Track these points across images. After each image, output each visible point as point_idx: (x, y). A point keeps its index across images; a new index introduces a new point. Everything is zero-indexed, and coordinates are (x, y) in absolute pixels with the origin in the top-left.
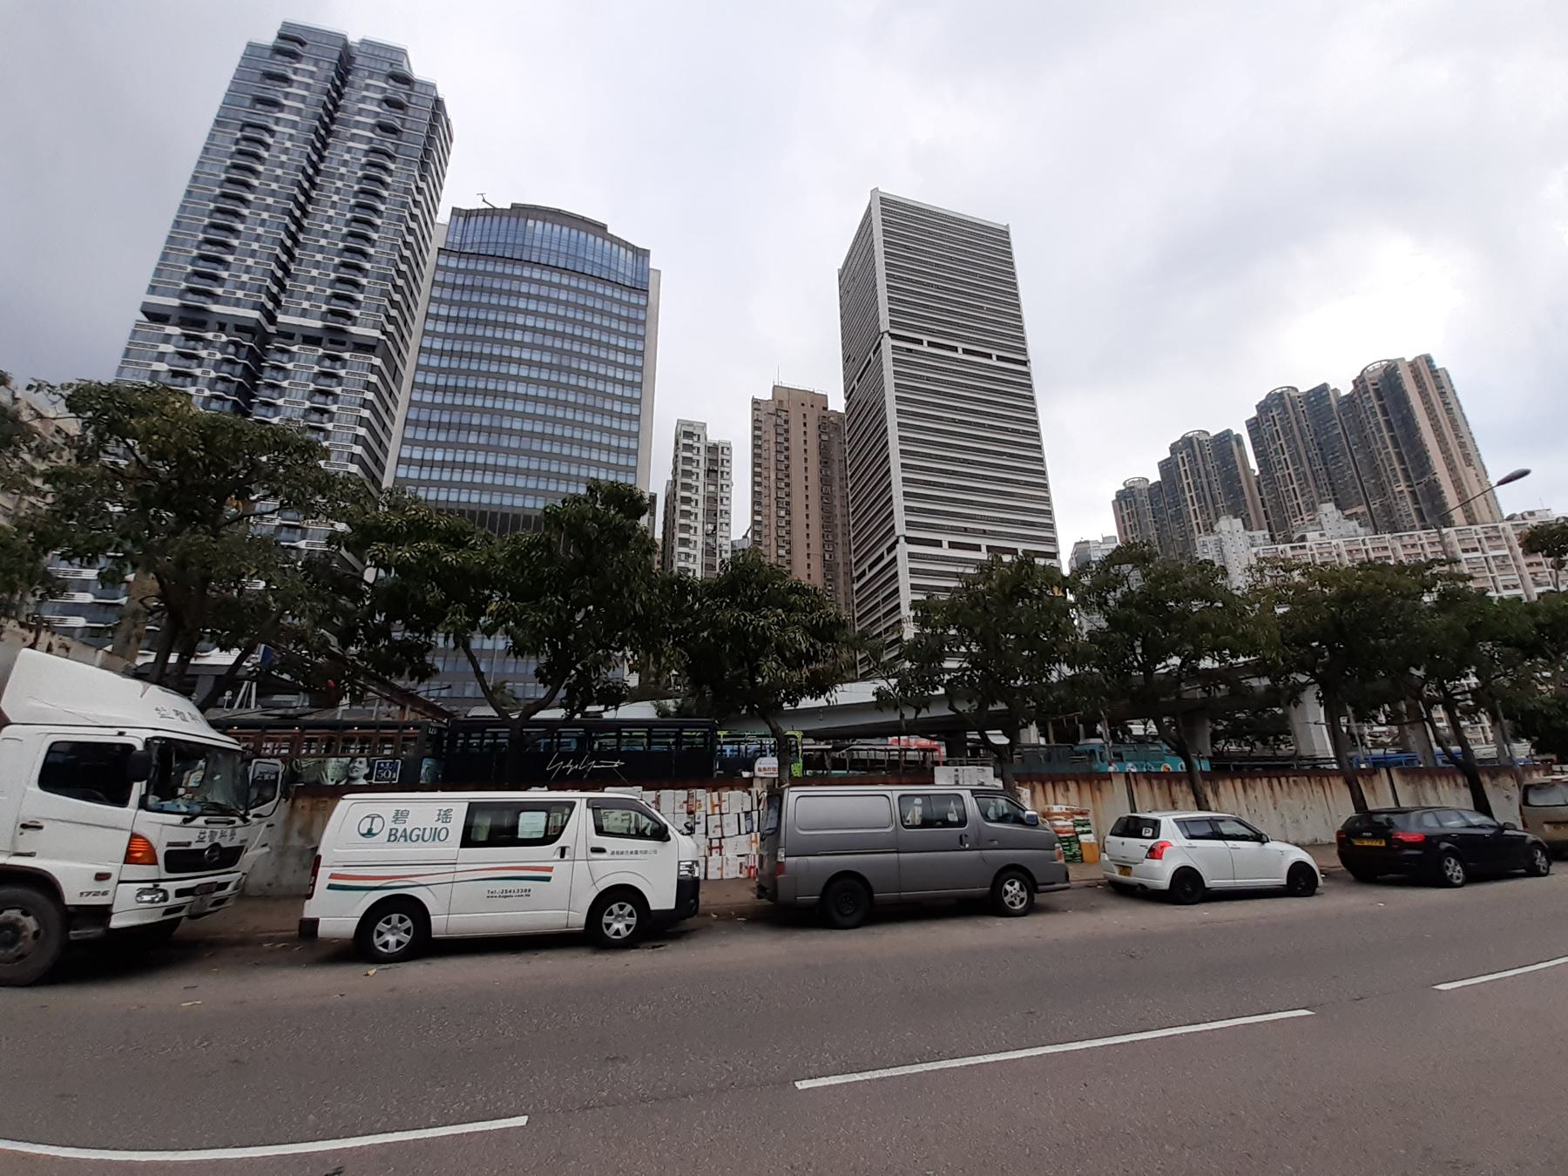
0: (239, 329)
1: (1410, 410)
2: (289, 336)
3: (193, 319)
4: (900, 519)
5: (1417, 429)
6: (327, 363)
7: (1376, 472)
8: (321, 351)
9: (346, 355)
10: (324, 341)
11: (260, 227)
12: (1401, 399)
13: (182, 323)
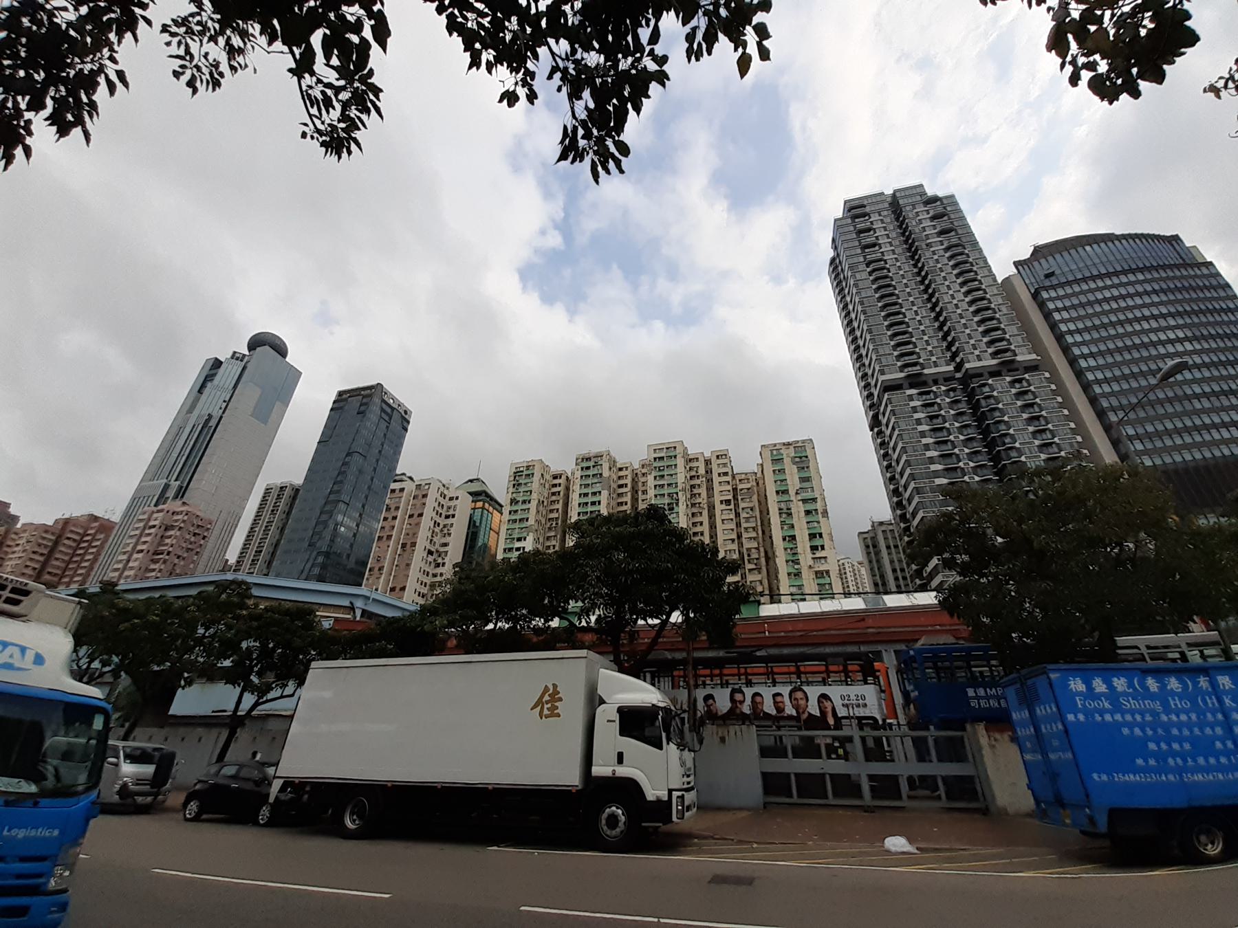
0: (946, 380)
2: (981, 375)
3: (916, 381)
6: (1017, 385)
8: (1008, 379)
9: (1026, 376)
13: (912, 386)
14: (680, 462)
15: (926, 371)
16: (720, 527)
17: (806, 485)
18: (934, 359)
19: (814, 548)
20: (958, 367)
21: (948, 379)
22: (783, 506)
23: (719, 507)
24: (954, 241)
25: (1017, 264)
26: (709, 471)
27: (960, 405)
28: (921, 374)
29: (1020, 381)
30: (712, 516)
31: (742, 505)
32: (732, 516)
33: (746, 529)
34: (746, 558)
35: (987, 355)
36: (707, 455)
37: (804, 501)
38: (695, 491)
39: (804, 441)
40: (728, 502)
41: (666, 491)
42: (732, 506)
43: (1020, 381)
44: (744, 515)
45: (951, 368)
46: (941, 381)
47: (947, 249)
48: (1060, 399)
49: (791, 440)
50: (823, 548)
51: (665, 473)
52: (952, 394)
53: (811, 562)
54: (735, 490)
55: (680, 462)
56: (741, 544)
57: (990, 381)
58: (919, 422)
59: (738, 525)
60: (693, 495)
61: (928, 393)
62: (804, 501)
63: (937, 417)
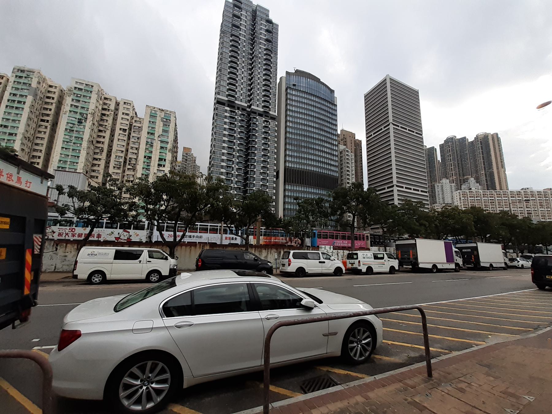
1: (490, 149)
2: (255, 113)
3: (231, 104)
4: (395, 180)
5: (491, 155)
7: (476, 166)
9: (270, 121)
10: (264, 116)
11: (242, 74)
12: (488, 146)
13: (228, 106)
14: (94, 96)
15: (236, 102)
16: (115, 142)
17: (164, 134)
18: (241, 98)
19: (159, 165)
20: (249, 107)
21: (244, 110)
22: (149, 140)
23: (117, 132)
24: (270, 48)
25: (287, 73)
26: (117, 109)
27: (243, 123)
28: (234, 102)
29: (267, 122)
30: (112, 135)
31: (133, 134)
32: (126, 138)
33: (132, 148)
34: (128, 162)
35: (261, 106)
36: (119, 100)
37: (162, 142)
38: (105, 118)
39: (171, 112)
40: (125, 130)
41: (79, 110)
42: (127, 133)
43: (267, 122)
44: (132, 140)
45: (246, 105)
46: (241, 109)
47: (266, 49)
48: (276, 134)
49: (164, 109)
50: (164, 166)
51: (81, 99)
52: (242, 116)
53: (156, 171)
54: (131, 125)
55: (94, 96)
56: (126, 155)
57: (257, 117)
58: (225, 123)
59: (128, 144)
60: (102, 120)
61: (234, 112)
62: (162, 142)
63: (233, 124)
